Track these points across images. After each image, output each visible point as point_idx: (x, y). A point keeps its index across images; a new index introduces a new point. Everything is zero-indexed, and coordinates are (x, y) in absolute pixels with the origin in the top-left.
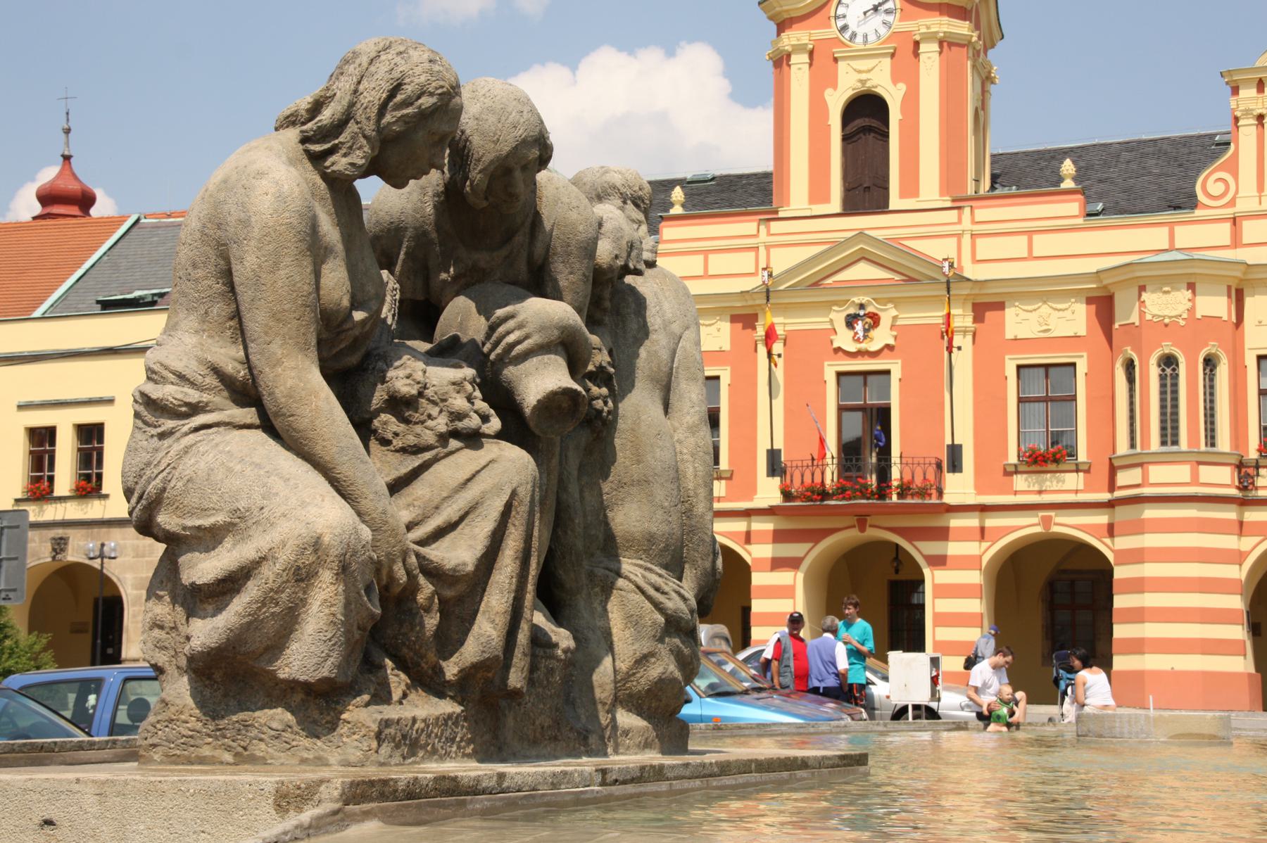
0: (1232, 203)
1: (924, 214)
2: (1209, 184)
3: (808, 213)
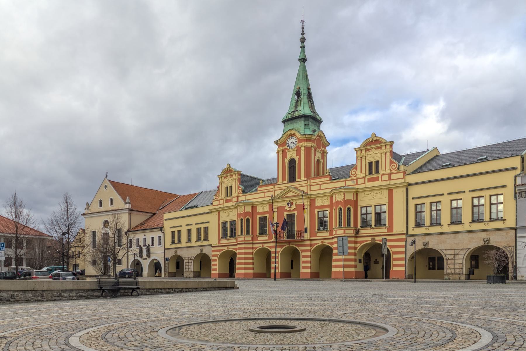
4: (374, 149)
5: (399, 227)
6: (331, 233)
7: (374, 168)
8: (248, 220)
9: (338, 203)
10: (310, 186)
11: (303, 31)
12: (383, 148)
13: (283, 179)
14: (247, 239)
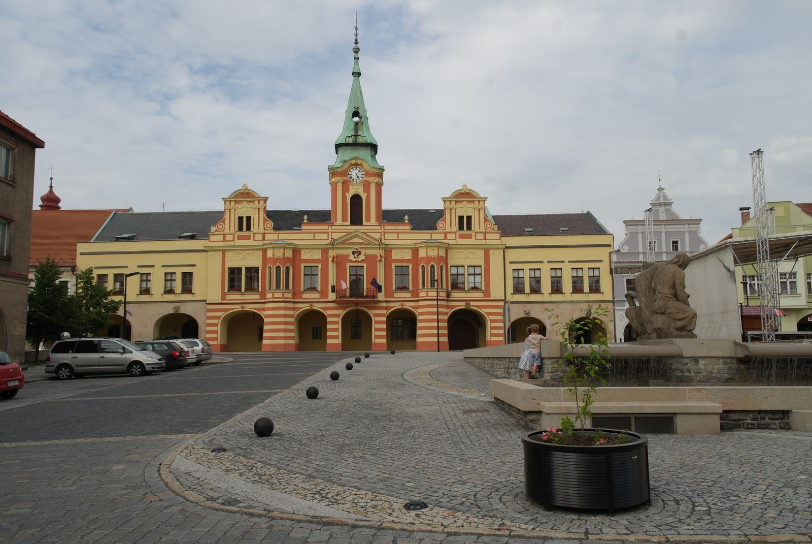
0: (445, 229)
1: (371, 225)
2: (440, 224)
3: (342, 224)
4: (245, 202)
5: (497, 292)
6: (263, 295)
7: (245, 224)
8: (287, 268)
9: (275, 260)
10: (384, 233)
11: (356, 40)
12: (256, 202)
13: (344, 219)
14: (430, 294)
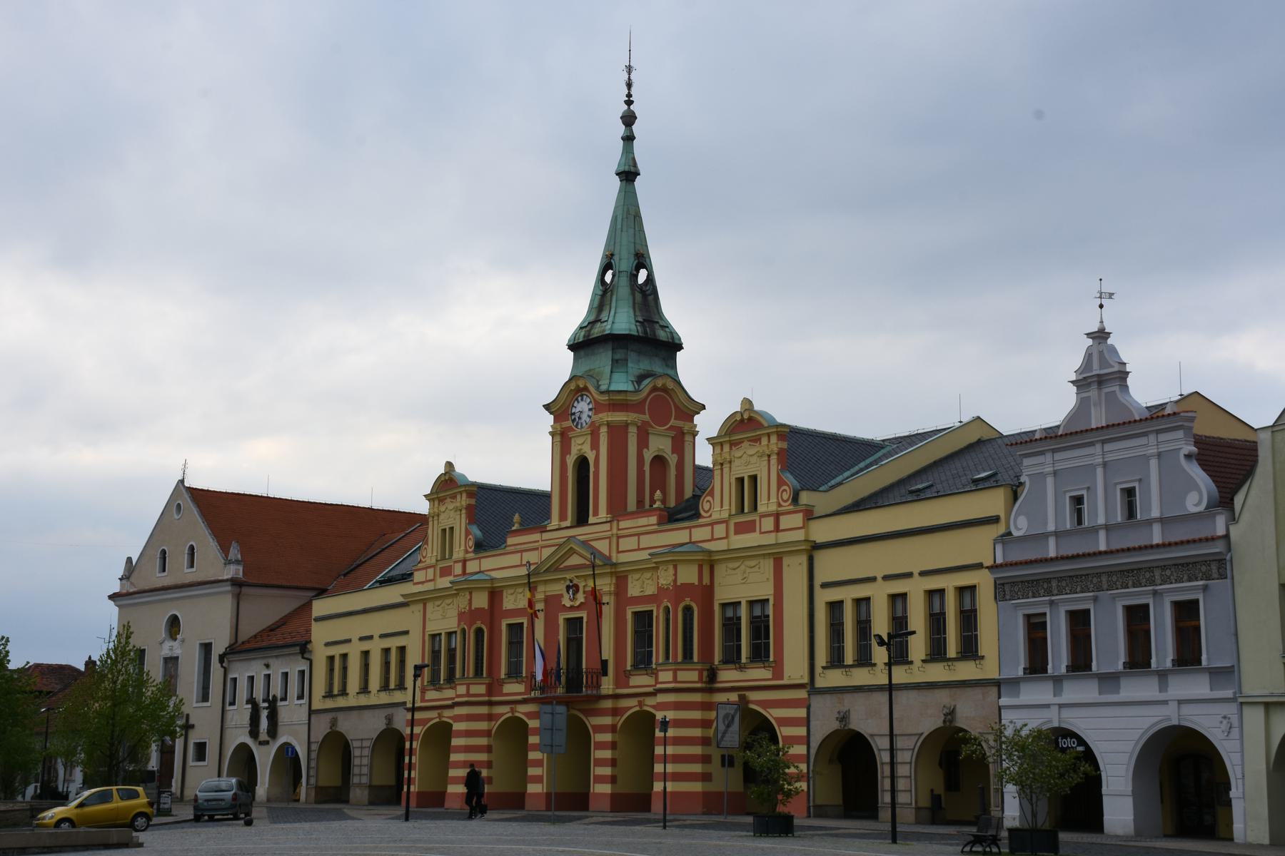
8: (479, 632)
11: (629, 95)
